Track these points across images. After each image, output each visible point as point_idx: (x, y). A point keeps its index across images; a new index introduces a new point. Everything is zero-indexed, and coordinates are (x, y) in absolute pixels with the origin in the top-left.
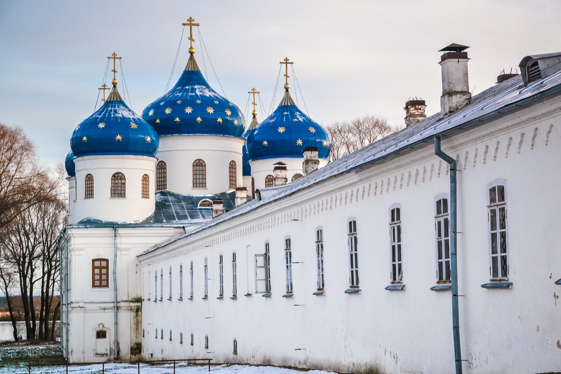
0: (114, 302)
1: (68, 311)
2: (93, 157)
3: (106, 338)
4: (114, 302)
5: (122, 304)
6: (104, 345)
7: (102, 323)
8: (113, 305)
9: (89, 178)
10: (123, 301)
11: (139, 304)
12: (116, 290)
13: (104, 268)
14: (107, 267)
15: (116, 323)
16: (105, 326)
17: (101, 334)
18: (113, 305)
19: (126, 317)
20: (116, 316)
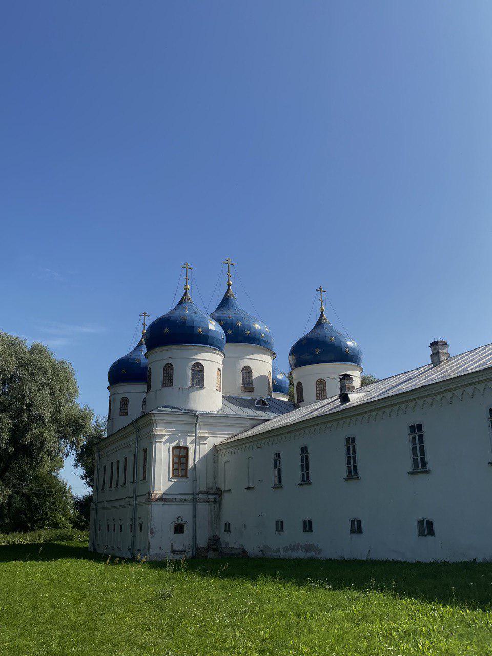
0: (193, 494)
1: (136, 503)
2: (174, 347)
3: (183, 533)
4: (193, 494)
5: (201, 496)
6: (182, 541)
7: (179, 517)
8: (191, 496)
9: (169, 368)
10: (201, 492)
11: (216, 496)
12: (195, 479)
13: (182, 456)
14: (186, 456)
15: (195, 517)
16: (184, 519)
17: (179, 529)
18: (191, 496)
19: (204, 509)
20: (195, 509)
